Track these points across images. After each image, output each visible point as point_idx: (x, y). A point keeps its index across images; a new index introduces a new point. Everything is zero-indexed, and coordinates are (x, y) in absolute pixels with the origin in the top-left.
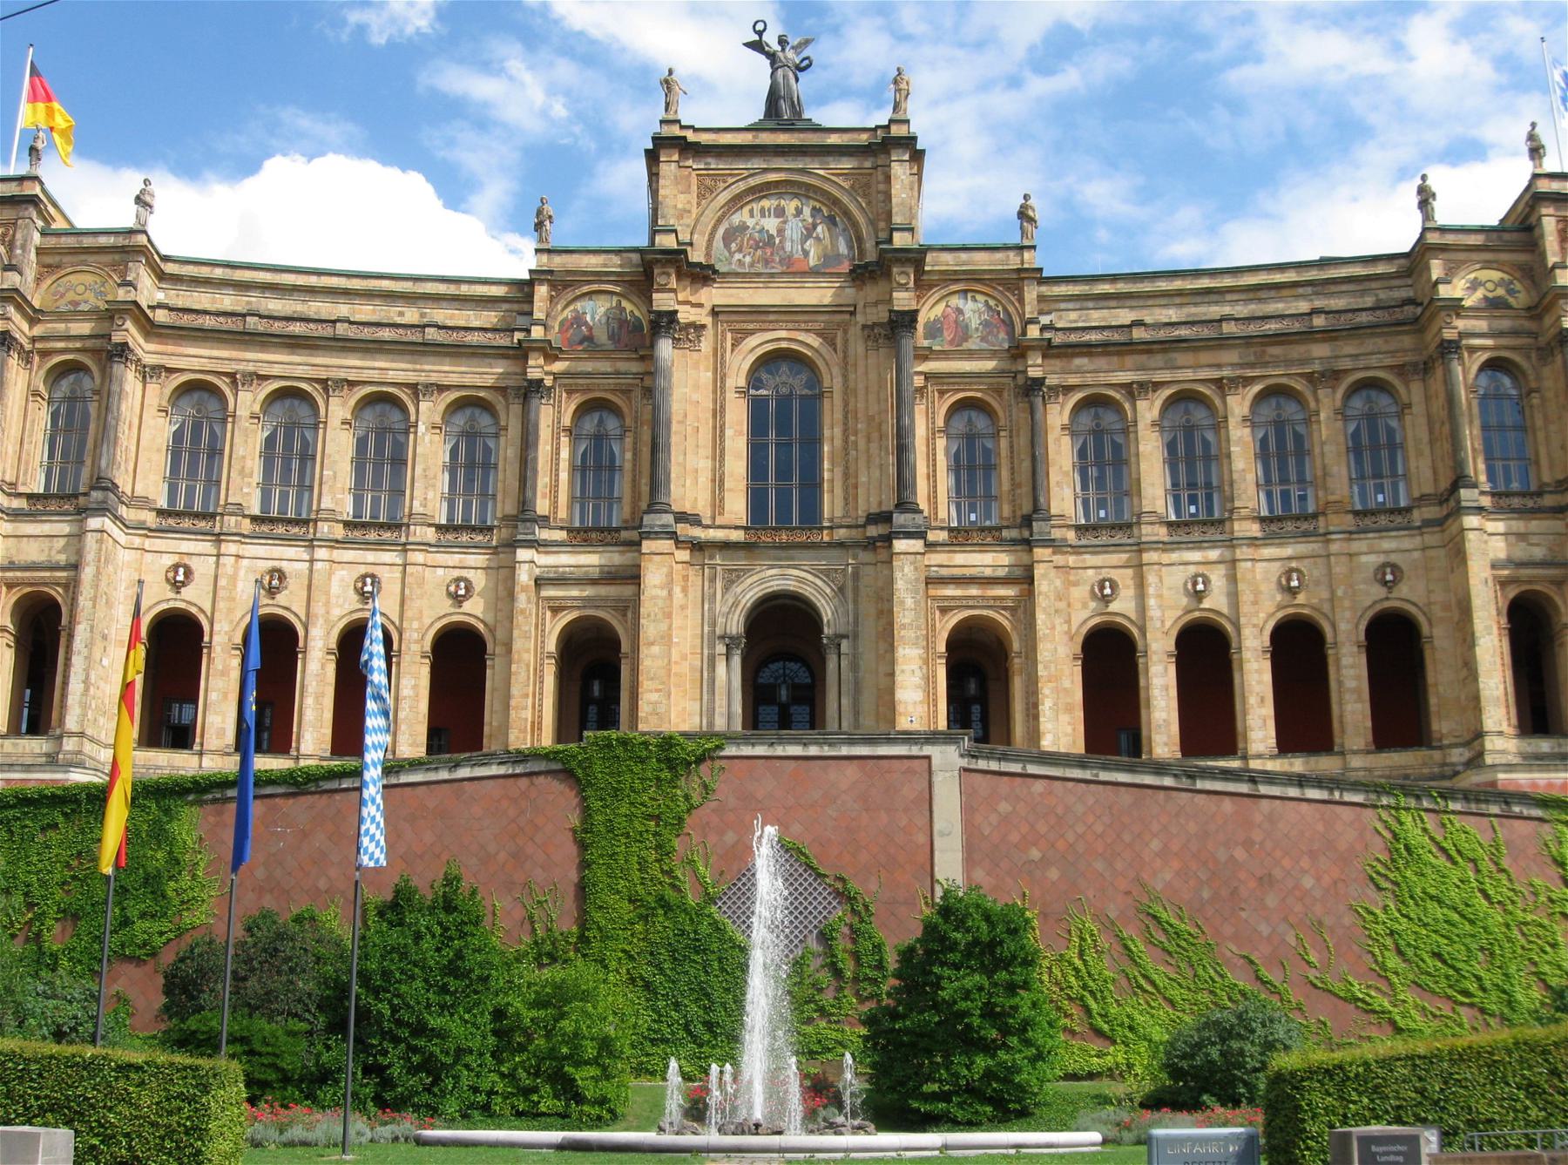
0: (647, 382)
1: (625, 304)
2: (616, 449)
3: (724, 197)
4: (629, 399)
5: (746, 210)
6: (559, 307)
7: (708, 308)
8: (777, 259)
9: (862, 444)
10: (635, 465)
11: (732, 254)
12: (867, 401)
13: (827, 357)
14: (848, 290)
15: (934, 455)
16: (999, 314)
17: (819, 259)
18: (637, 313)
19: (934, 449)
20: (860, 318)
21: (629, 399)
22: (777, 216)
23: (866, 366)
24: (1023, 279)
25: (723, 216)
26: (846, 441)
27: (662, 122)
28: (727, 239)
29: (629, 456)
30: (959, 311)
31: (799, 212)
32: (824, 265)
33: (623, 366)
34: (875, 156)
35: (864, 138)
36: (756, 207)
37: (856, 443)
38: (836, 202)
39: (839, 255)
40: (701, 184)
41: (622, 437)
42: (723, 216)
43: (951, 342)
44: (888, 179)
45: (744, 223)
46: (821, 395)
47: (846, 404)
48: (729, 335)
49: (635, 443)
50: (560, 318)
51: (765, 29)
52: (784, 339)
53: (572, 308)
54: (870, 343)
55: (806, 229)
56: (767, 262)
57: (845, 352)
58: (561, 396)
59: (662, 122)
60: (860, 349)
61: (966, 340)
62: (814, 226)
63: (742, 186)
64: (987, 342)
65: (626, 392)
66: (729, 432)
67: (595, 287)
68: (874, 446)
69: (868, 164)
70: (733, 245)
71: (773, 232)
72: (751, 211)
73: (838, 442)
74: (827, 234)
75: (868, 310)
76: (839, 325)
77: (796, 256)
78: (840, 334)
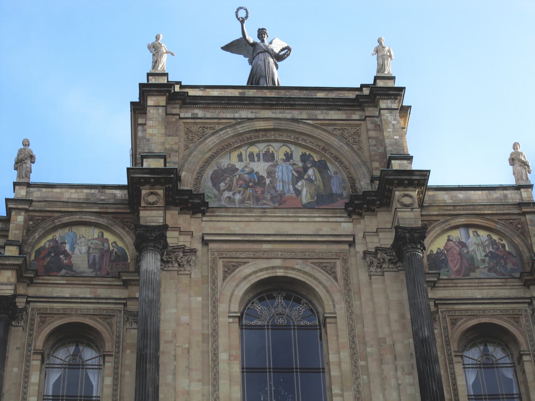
0: (132, 306)
1: (107, 235)
2: (93, 378)
3: (212, 141)
4: (110, 325)
5: (235, 155)
6: (37, 235)
7: (198, 235)
8: (269, 197)
9: (373, 366)
10: (115, 390)
11: (221, 192)
12: (375, 326)
13: (328, 284)
14: (343, 224)
15: (454, 379)
16: (504, 246)
17: (312, 197)
18: (120, 244)
19: (453, 373)
20: (360, 248)
21: (110, 325)
22: (265, 160)
23: (371, 294)
24: (524, 214)
25: (212, 158)
26: (355, 364)
27: (149, 75)
28: (216, 179)
29: (108, 381)
30: (463, 245)
31: (288, 157)
32: (317, 202)
33: (103, 292)
34: (363, 110)
35: (351, 95)
36: (245, 151)
37: (366, 368)
38: (326, 148)
39: (332, 194)
40: (188, 131)
41: (100, 368)
42: (212, 158)
43: (458, 272)
44: (379, 128)
45: (233, 166)
46: (323, 324)
47: (351, 329)
48: (220, 263)
49: (116, 368)
50: (37, 248)
51: (247, 17)
52: (279, 267)
53: (50, 237)
54: (372, 269)
55: (297, 172)
56: (257, 200)
57: (347, 280)
58: (33, 320)
59: (149, 75)
60: (364, 276)
61: (474, 271)
62: (305, 169)
63: (230, 132)
64: (496, 272)
65: (107, 317)
66: (223, 356)
67: (77, 218)
68: (388, 369)
69: (356, 116)
70: (222, 185)
71: (265, 175)
72: (240, 157)
73: (346, 366)
74: (318, 176)
75: (368, 239)
76: (337, 256)
77: (288, 195)
78: (339, 263)
